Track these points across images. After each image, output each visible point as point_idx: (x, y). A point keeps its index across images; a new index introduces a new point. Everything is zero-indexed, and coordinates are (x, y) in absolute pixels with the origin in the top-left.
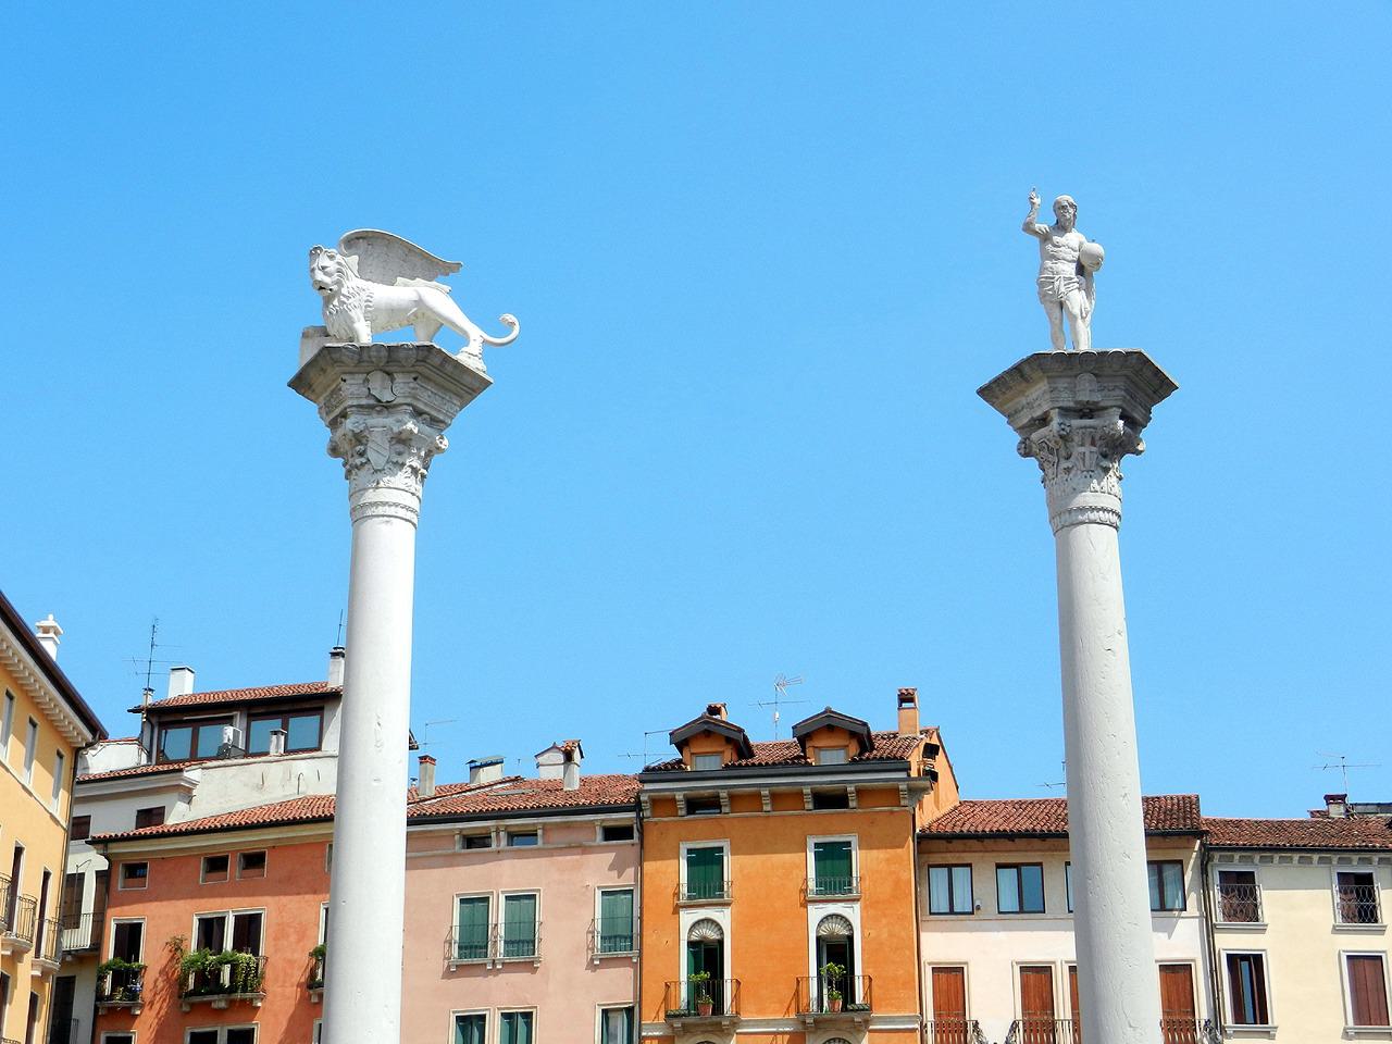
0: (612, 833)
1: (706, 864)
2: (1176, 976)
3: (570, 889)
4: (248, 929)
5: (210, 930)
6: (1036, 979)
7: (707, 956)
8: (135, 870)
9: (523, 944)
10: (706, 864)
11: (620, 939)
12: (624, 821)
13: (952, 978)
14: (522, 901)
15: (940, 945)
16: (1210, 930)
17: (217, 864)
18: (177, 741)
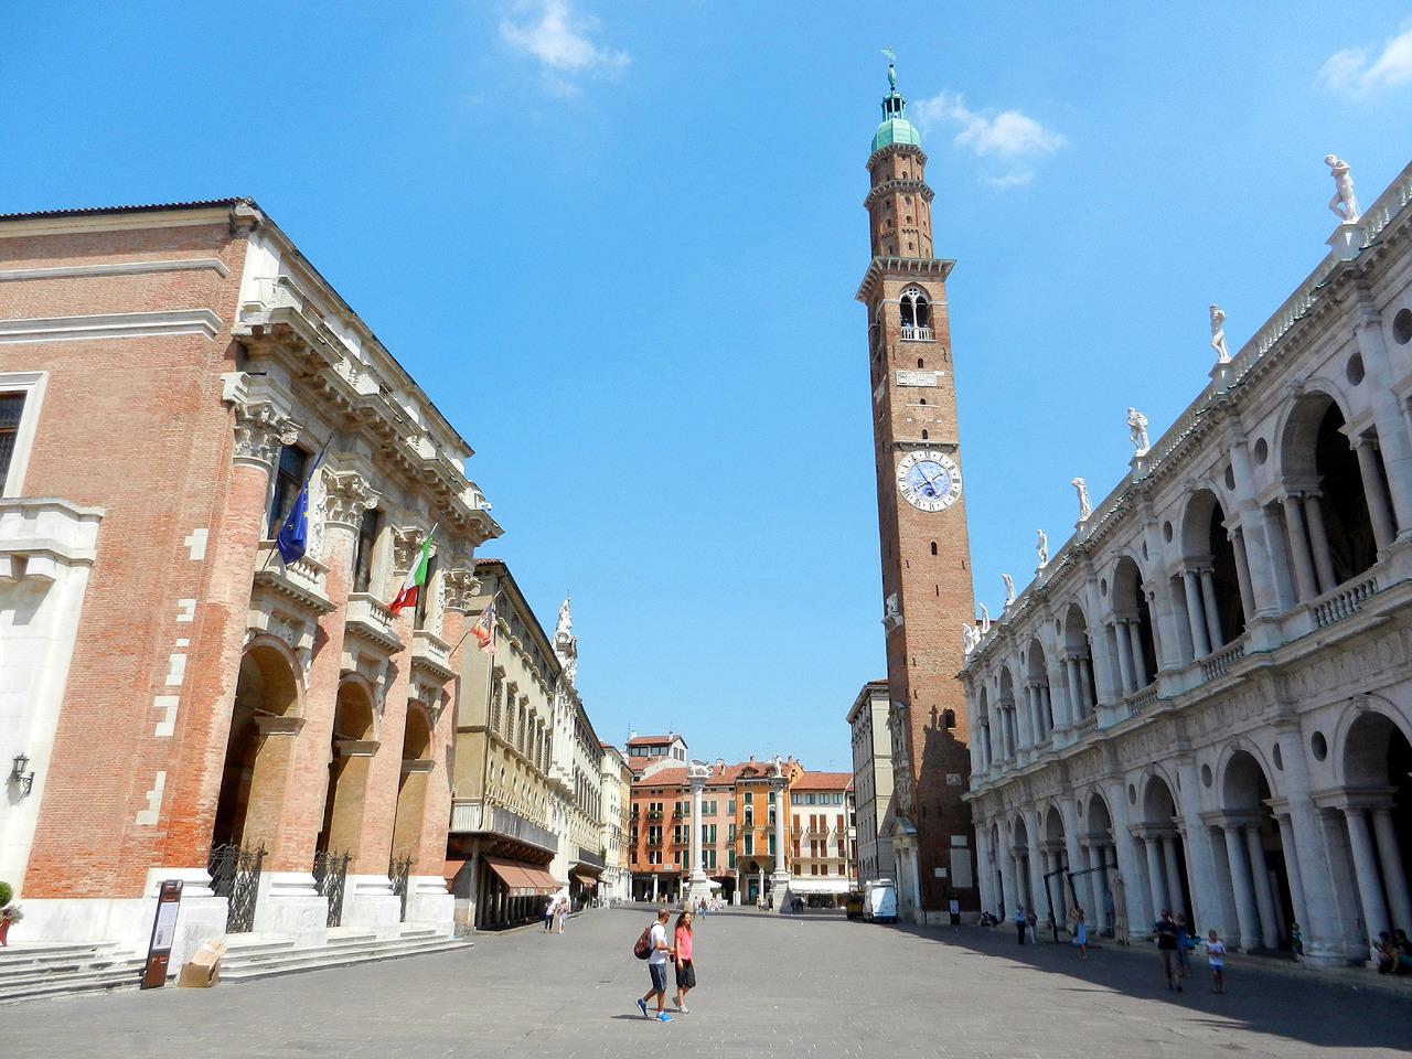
0: (730, 789)
1: (748, 797)
2: (840, 818)
3: (723, 800)
4: (660, 806)
5: (653, 806)
6: (813, 818)
7: (749, 814)
8: (636, 792)
9: (714, 811)
10: (748, 797)
11: (732, 810)
12: (734, 789)
13: (797, 818)
14: (714, 803)
15: (795, 810)
16: (847, 807)
17: (653, 792)
18: (635, 751)
